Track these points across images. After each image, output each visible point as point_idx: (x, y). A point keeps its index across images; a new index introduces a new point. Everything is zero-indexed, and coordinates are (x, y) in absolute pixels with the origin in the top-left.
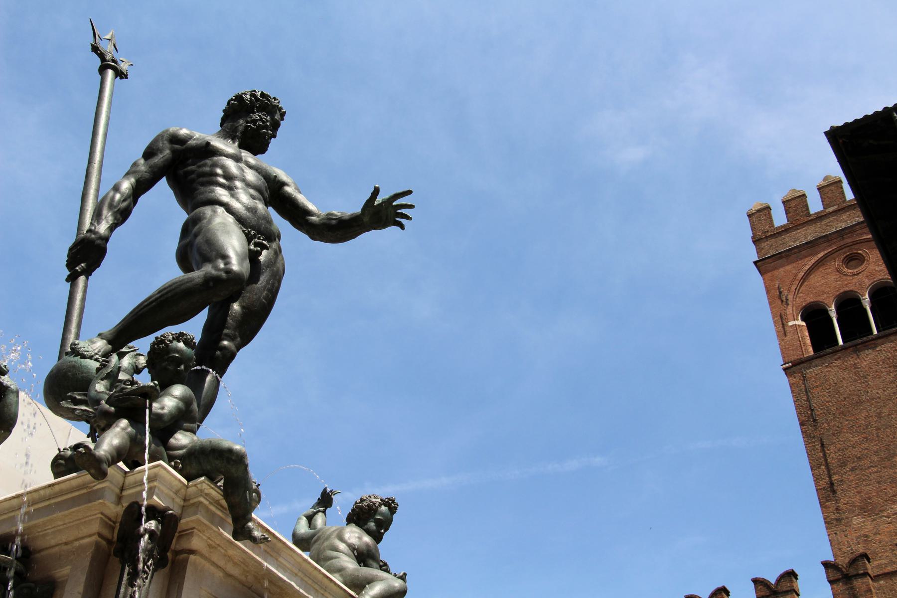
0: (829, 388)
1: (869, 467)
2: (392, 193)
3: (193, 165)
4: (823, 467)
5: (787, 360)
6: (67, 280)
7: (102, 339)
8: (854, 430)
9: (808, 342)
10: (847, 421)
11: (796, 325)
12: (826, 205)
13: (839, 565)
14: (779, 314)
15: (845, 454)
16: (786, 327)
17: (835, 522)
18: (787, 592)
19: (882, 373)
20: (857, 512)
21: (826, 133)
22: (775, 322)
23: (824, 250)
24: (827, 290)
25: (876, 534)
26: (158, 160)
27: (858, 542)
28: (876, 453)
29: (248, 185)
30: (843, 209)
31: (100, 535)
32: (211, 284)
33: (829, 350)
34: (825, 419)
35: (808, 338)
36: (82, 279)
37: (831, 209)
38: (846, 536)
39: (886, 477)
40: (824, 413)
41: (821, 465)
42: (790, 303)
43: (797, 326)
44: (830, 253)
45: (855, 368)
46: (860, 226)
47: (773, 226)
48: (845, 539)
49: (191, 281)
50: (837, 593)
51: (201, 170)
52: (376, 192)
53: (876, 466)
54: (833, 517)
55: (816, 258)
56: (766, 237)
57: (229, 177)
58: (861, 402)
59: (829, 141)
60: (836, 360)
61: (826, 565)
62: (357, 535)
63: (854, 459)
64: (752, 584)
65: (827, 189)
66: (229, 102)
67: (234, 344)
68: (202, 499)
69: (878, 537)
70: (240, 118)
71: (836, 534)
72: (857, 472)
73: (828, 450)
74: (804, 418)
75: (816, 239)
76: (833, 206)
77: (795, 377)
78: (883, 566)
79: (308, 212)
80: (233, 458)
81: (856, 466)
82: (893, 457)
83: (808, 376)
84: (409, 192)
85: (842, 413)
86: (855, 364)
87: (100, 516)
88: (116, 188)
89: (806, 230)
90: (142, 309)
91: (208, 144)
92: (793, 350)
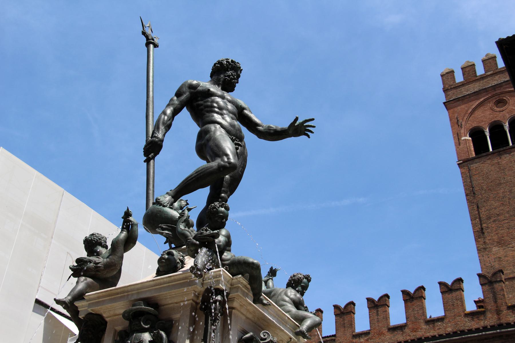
0: (483, 176)
1: (503, 220)
4: (478, 219)
6: (145, 161)
7: (169, 195)
8: (496, 199)
9: (472, 149)
10: (492, 194)
11: (466, 139)
12: (487, 70)
13: (486, 275)
14: (456, 133)
15: (490, 213)
16: (460, 141)
17: (483, 250)
18: (457, 290)
20: (495, 244)
21: (497, 42)
22: (454, 137)
23: (484, 97)
24: (485, 119)
25: (505, 257)
26: (183, 97)
27: (495, 261)
28: (508, 212)
29: (230, 112)
30: (496, 73)
31: (193, 300)
32: (222, 169)
33: (484, 154)
34: (480, 193)
35: (473, 147)
36: (152, 161)
37: (489, 73)
38: (489, 258)
39: (512, 226)
40: (480, 189)
41: (476, 218)
42: (463, 127)
43: (467, 140)
44: (487, 99)
45: (498, 164)
46: (506, 83)
47: (455, 82)
48: (488, 259)
49: (212, 168)
50: (485, 291)
51: (206, 104)
52: (297, 119)
53: (507, 220)
54: (482, 247)
55: (479, 101)
56: (451, 88)
57: (220, 108)
58: (501, 184)
59: (498, 47)
60: (488, 159)
61: (479, 275)
62: (294, 294)
63: (495, 215)
64: (438, 285)
66: (215, 64)
67: (227, 196)
68: (240, 285)
69: (506, 258)
70: (221, 74)
71: (483, 256)
72: (497, 223)
73: (481, 210)
74: (468, 192)
75: (480, 91)
77: (464, 169)
78: (508, 274)
79: (257, 125)
80: (255, 267)
81: (496, 219)
83: (471, 168)
84: (313, 119)
85: (490, 190)
86: (499, 162)
87: (193, 292)
88: (164, 113)
89: (474, 85)
90: (188, 181)
91: (209, 90)
92: (463, 153)
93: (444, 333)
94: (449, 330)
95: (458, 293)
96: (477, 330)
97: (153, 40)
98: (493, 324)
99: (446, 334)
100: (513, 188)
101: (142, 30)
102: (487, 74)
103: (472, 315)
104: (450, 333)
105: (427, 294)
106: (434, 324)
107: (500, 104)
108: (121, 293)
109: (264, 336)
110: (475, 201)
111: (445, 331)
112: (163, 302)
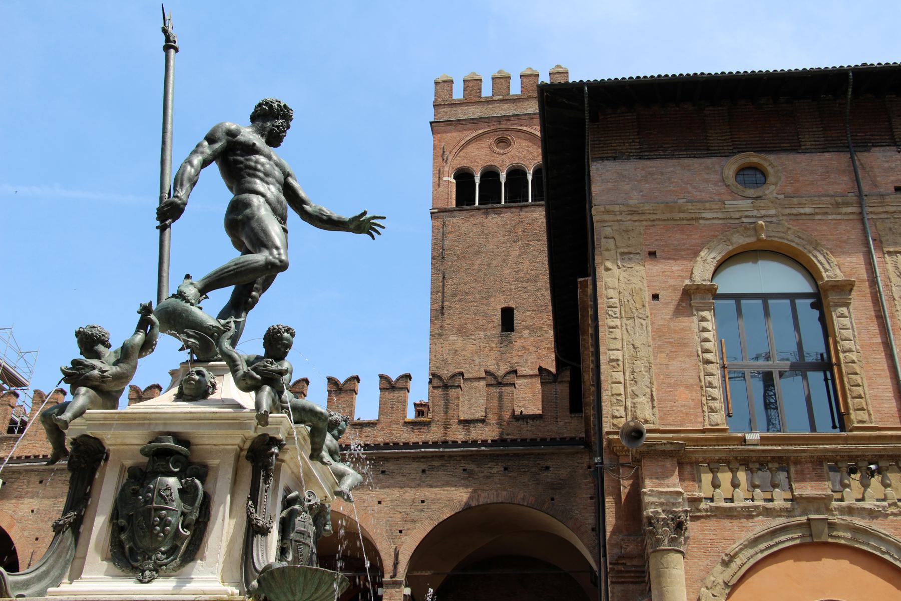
1: (472, 301)
2: (372, 215)
5: (435, 207)
6: (157, 228)
9: (454, 196)
12: (495, 93)
17: (437, 336)
18: (402, 388)
19: (500, 234)
22: (434, 174)
23: (484, 128)
26: (217, 146)
33: (468, 207)
37: (497, 98)
39: (481, 311)
41: (439, 292)
44: (488, 132)
45: (482, 226)
46: (515, 117)
49: (257, 262)
51: (248, 163)
52: (365, 213)
54: (437, 332)
55: (476, 133)
56: (444, 105)
60: (471, 216)
65: (499, 81)
66: (260, 105)
70: (268, 120)
71: (436, 344)
72: (463, 303)
75: (481, 118)
76: (499, 95)
77: (438, 221)
79: (304, 202)
82: (490, 298)
84: (384, 218)
85: (464, 257)
86: (483, 223)
89: (475, 108)
90: (222, 274)
94: (380, 440)
95: (402, 393)
96: (416, 445)
97: (175, 42)
98: (436, 440)
100: (493, 262)
101: (162, 25)
102: (494, 98)
103: (413, 424)
105: (360, 387)
106: (361, 428)
107: (501, 144)
108: (139, 419)
109: (309, 496)
110: (442, 268)
112: (197, 441)
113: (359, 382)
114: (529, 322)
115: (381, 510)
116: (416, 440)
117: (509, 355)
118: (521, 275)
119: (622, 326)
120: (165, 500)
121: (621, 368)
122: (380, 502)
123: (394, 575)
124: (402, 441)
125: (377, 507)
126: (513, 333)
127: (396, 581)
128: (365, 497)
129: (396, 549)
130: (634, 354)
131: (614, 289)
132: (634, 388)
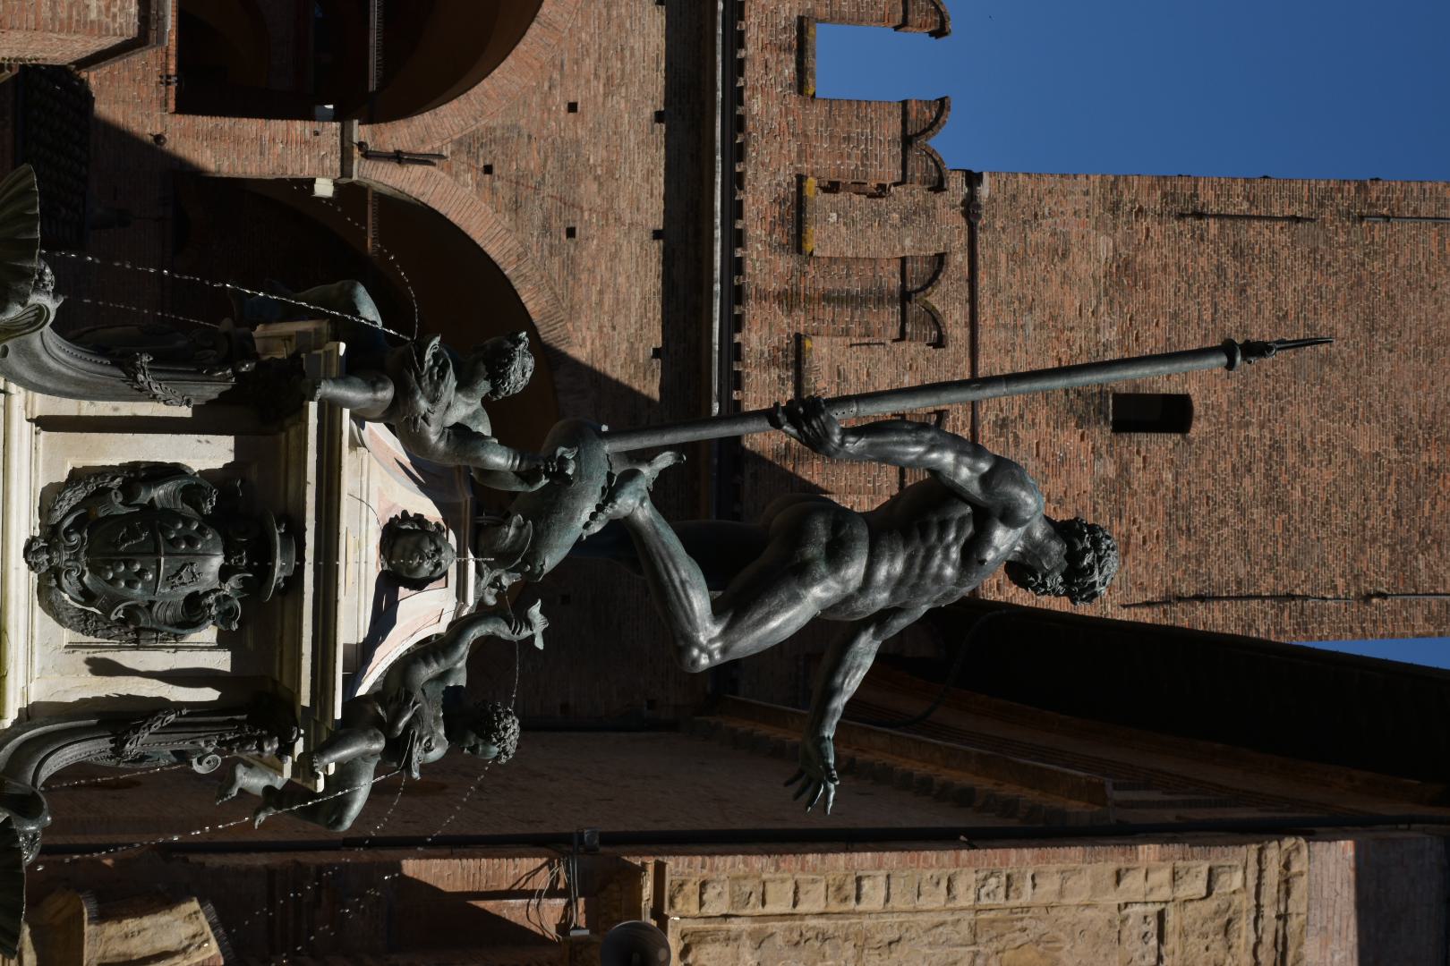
3: (956, 539)
8: (1311, 298)
10: (1338, 289)
13: (933, 288)
15: (1260, 262)
19: (1427, 394)
20: (1122, 250)
25: (1064, 276)
27: (1055, 234)
34: (1357, 243)
38: (1075, 212)
40: (1372, 243)
41: (1252, 203)
48: (1070, 209)
50: (878, 268)
53: (1213, 320)
54: (1126, 197)
58: (1372, 330)
63: (1244, 278)
69: (1057, 279)
71: (1087, 193)
72: (1212, 278)
73: (1282, 228)
74: (1374, 195)
78: (993, 271)
81: (1225, 278)
85: (1360, 282)
93: (745, 81)
94: (755, 105)
96: (734, 210)
98: (748, 270)
99: (741, 88)
104: (741, 103)
105: (917, 38)
110: (1327, 215)
111: (754, 89)
113: (932, 34)
114: (1140, 479)
115: (549, 110)
116: (750, 209)
117: (1041, 417)
118: (1291, 458)
119: (953, 911)
120: (173, 576)
121: (835, 906)
122: (572, 107)
123: (367, 155)
124: (749, 169)
125: (559, 101)
126: (1108, 430)
127: (351, 159)
128: (589, 64)
129: (440, 156)
130: (873, 943)
131: (1061, 893)
132: (779, 940)
